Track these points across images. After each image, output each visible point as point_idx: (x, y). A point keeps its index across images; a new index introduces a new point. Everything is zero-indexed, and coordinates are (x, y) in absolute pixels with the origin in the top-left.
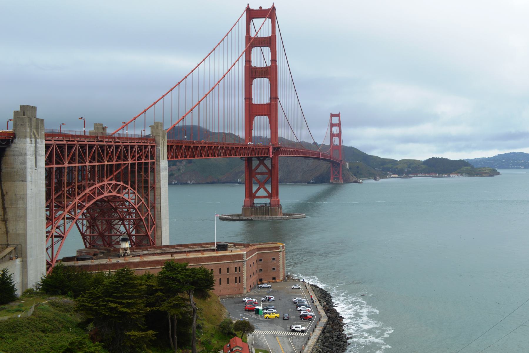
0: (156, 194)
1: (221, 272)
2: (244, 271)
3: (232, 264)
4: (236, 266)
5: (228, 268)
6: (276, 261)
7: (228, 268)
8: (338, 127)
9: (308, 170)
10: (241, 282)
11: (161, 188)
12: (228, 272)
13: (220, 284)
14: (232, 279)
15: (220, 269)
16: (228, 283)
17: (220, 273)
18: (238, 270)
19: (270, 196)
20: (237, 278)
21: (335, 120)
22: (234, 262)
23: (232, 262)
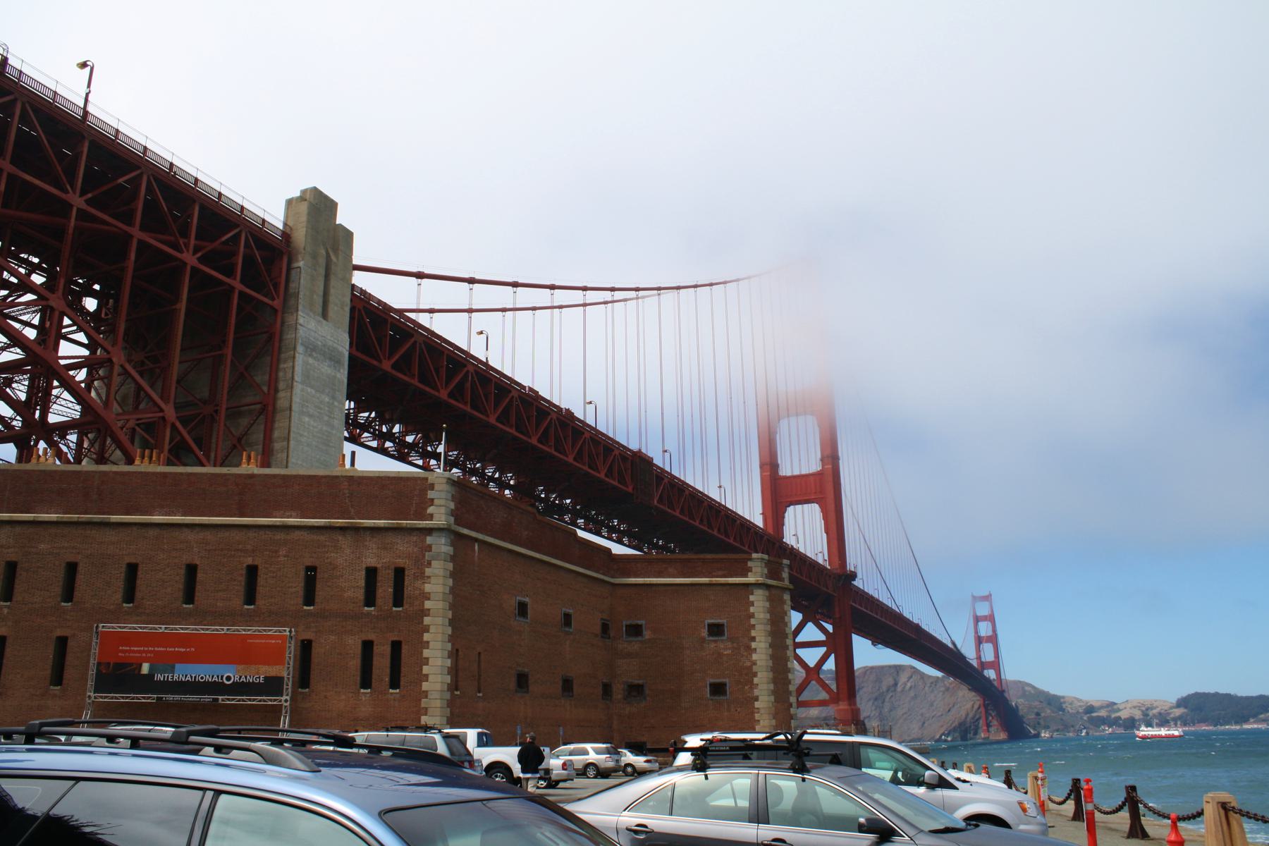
0: (276, 434)
1: (261, 589)
2: (428, 604)
4: (371, 561)
6: (730, 639)
8: (990, 623)
9: (933, 717)
10: (403, 681)
11: (295, 407)
12: (309, 599)
15: (252, 571)
18: (385, 590)
19: (834, 699)
20: (377, 649)
21: (983, 610)
22: (357, 529)
23: (343, 529)
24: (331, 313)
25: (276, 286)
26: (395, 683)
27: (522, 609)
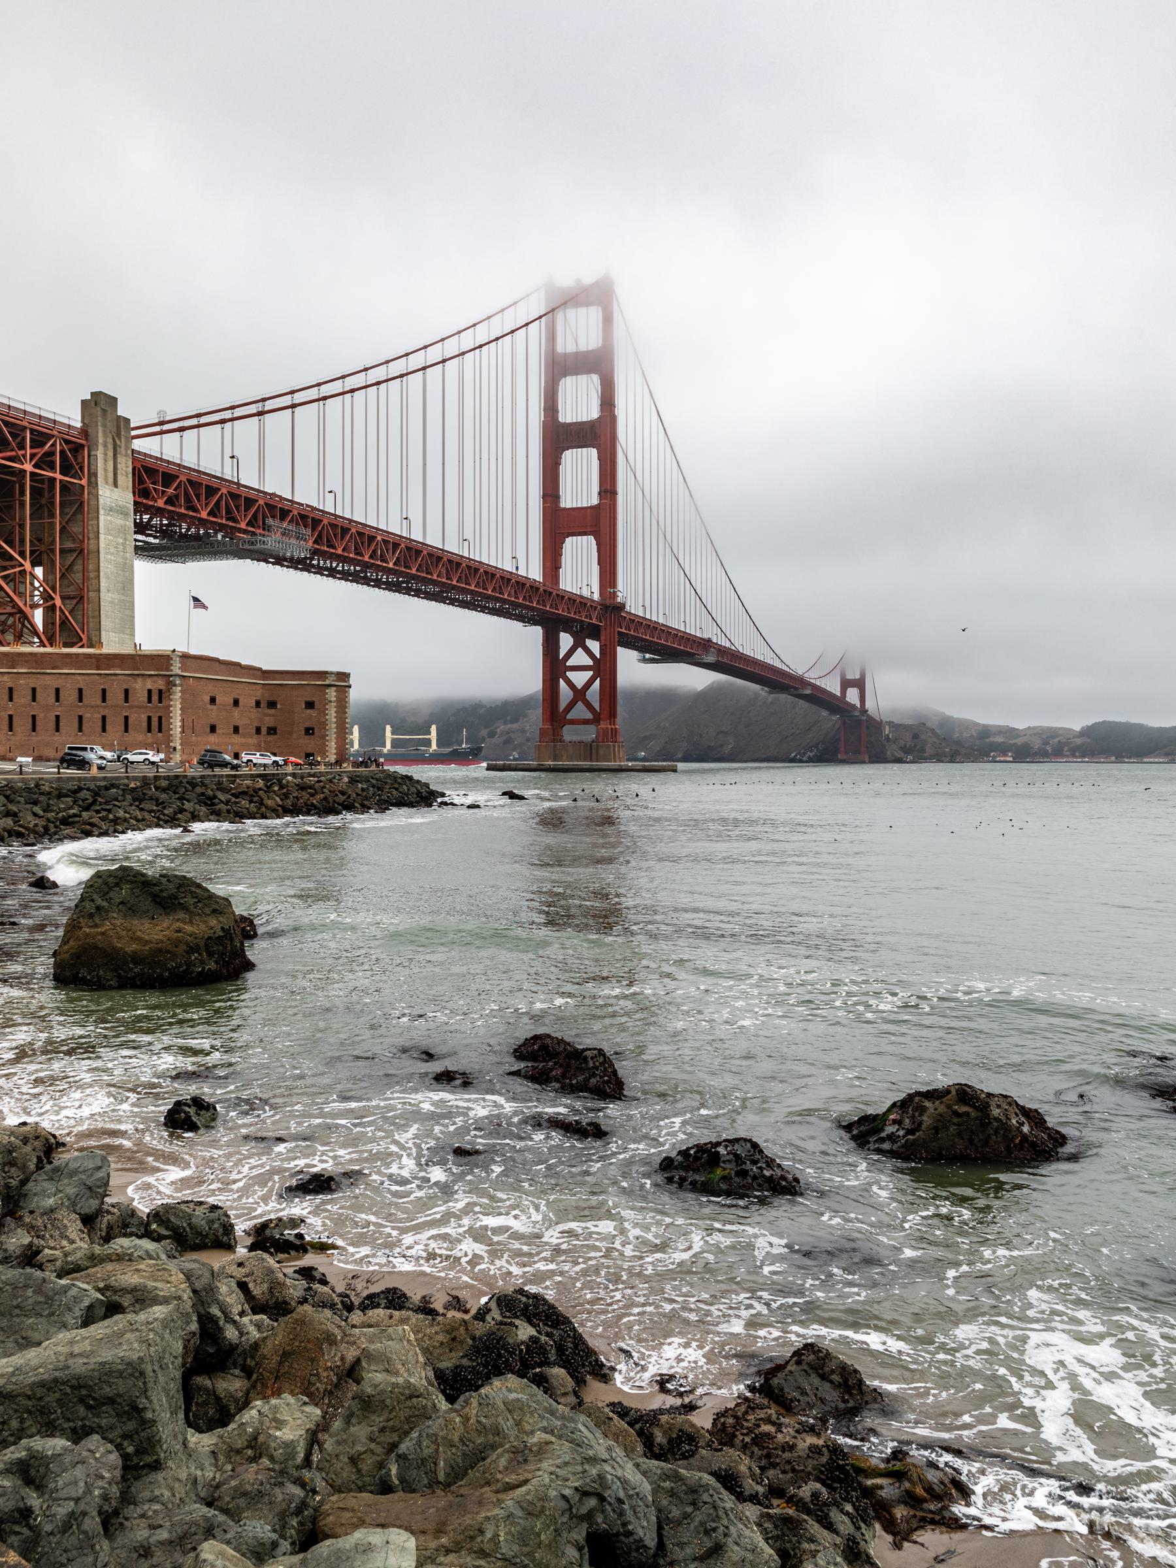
3: (139, 680)
4: (149, 687)
5: (127, 691)
7: (127, 691)
12: (126, 700)
13: (104, 730)
14: (138, 718)
15: (104, 691)
16: (126, 730)
17: (104, 700)
18: (155, 697)
22: (143, 675)
24: (119, 482)
25: (82, 469)
26: (160, 731)
27: (213, 700)
